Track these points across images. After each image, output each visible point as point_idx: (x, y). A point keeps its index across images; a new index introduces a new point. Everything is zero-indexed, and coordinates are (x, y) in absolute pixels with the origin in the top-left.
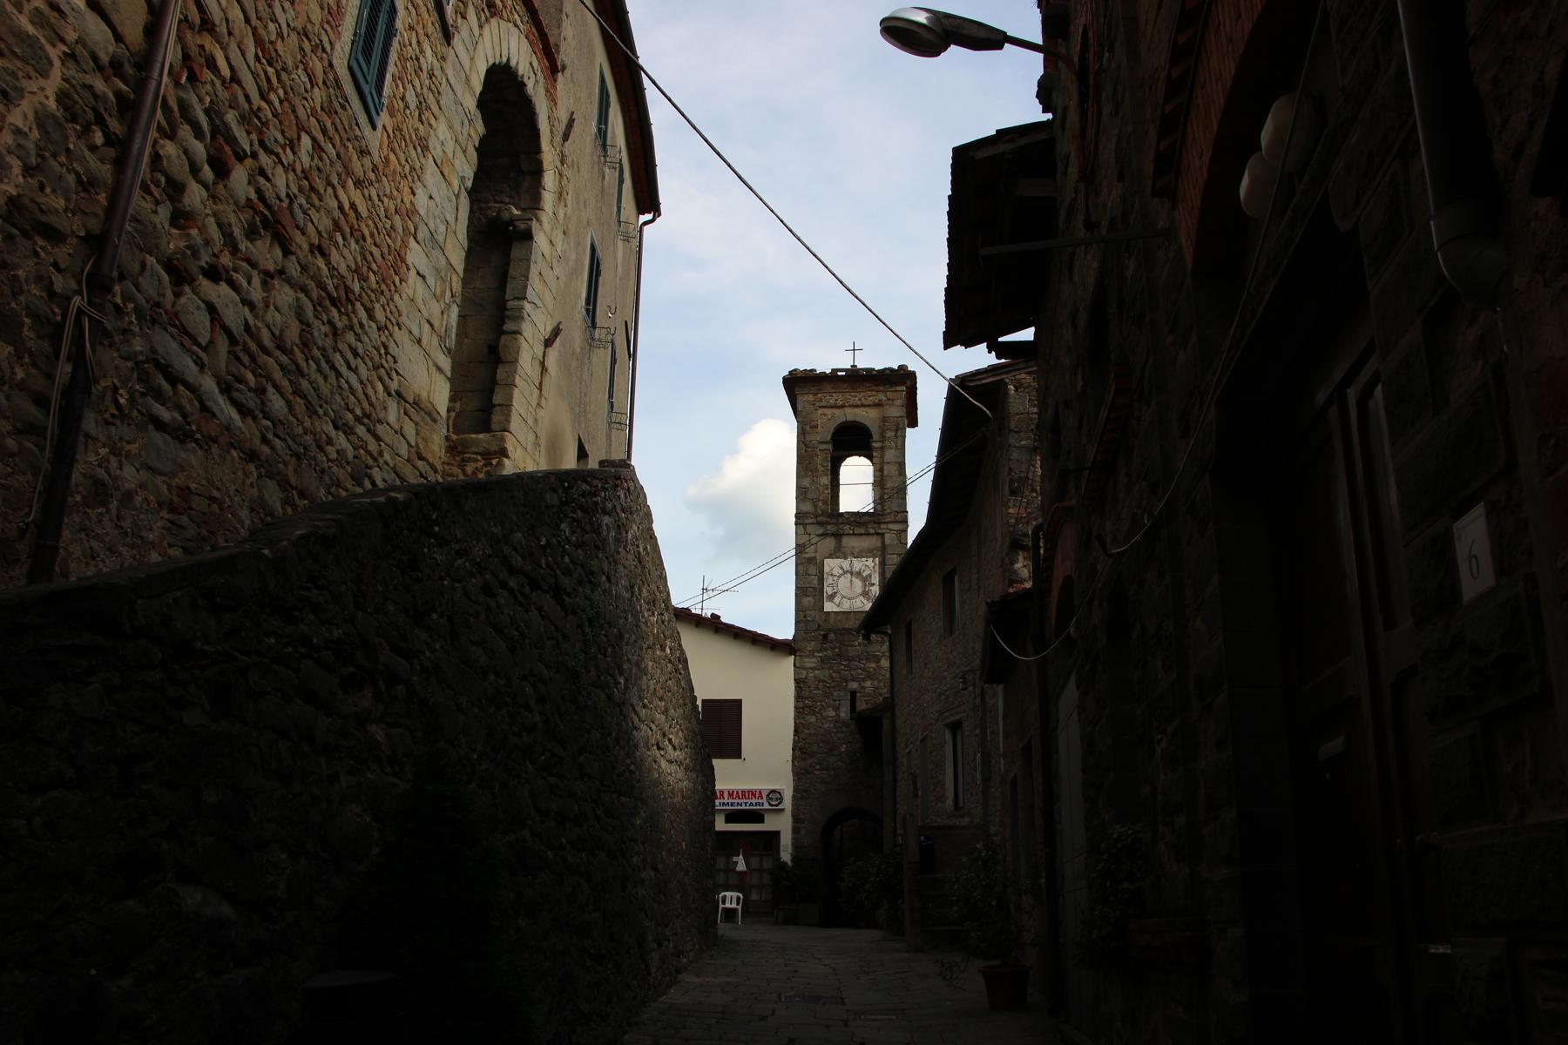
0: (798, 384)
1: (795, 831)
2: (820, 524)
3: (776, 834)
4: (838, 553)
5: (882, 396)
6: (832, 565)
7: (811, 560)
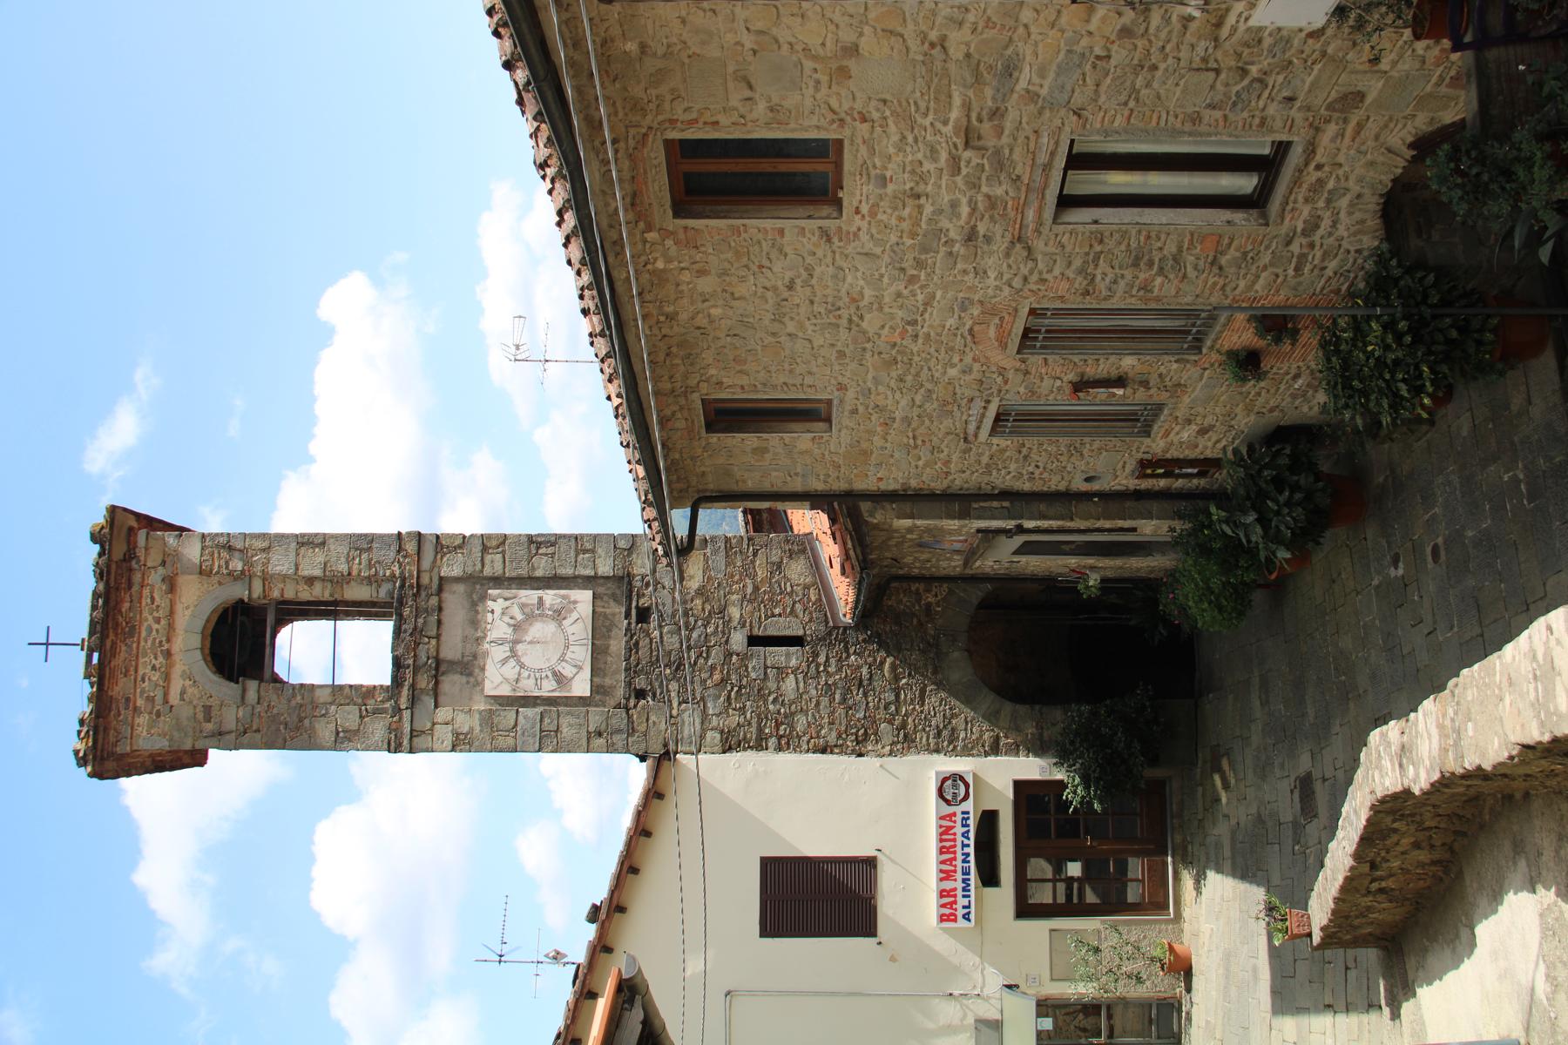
0: (108, 752)
1: (1014, 750)
2: (413, 701)
3: (1018, 785)
4: (469, 667)
5: (155, 578)
6: (497, 678)
7: (488, 719)
